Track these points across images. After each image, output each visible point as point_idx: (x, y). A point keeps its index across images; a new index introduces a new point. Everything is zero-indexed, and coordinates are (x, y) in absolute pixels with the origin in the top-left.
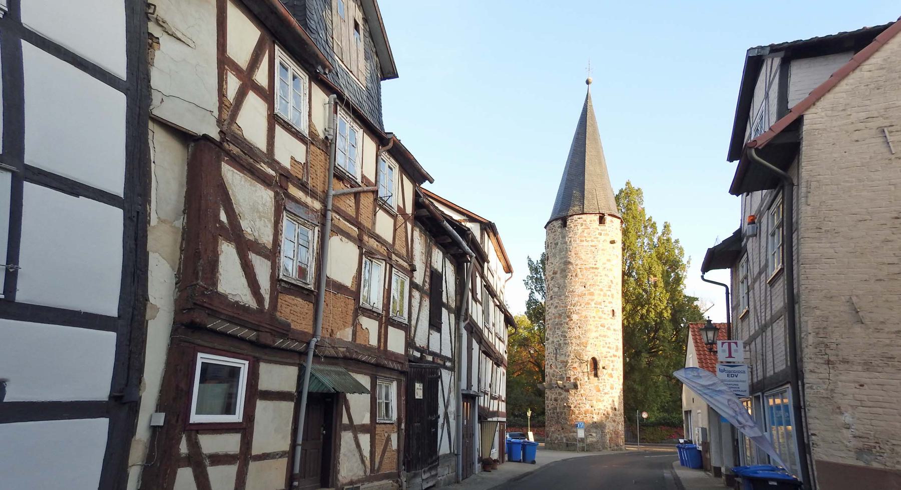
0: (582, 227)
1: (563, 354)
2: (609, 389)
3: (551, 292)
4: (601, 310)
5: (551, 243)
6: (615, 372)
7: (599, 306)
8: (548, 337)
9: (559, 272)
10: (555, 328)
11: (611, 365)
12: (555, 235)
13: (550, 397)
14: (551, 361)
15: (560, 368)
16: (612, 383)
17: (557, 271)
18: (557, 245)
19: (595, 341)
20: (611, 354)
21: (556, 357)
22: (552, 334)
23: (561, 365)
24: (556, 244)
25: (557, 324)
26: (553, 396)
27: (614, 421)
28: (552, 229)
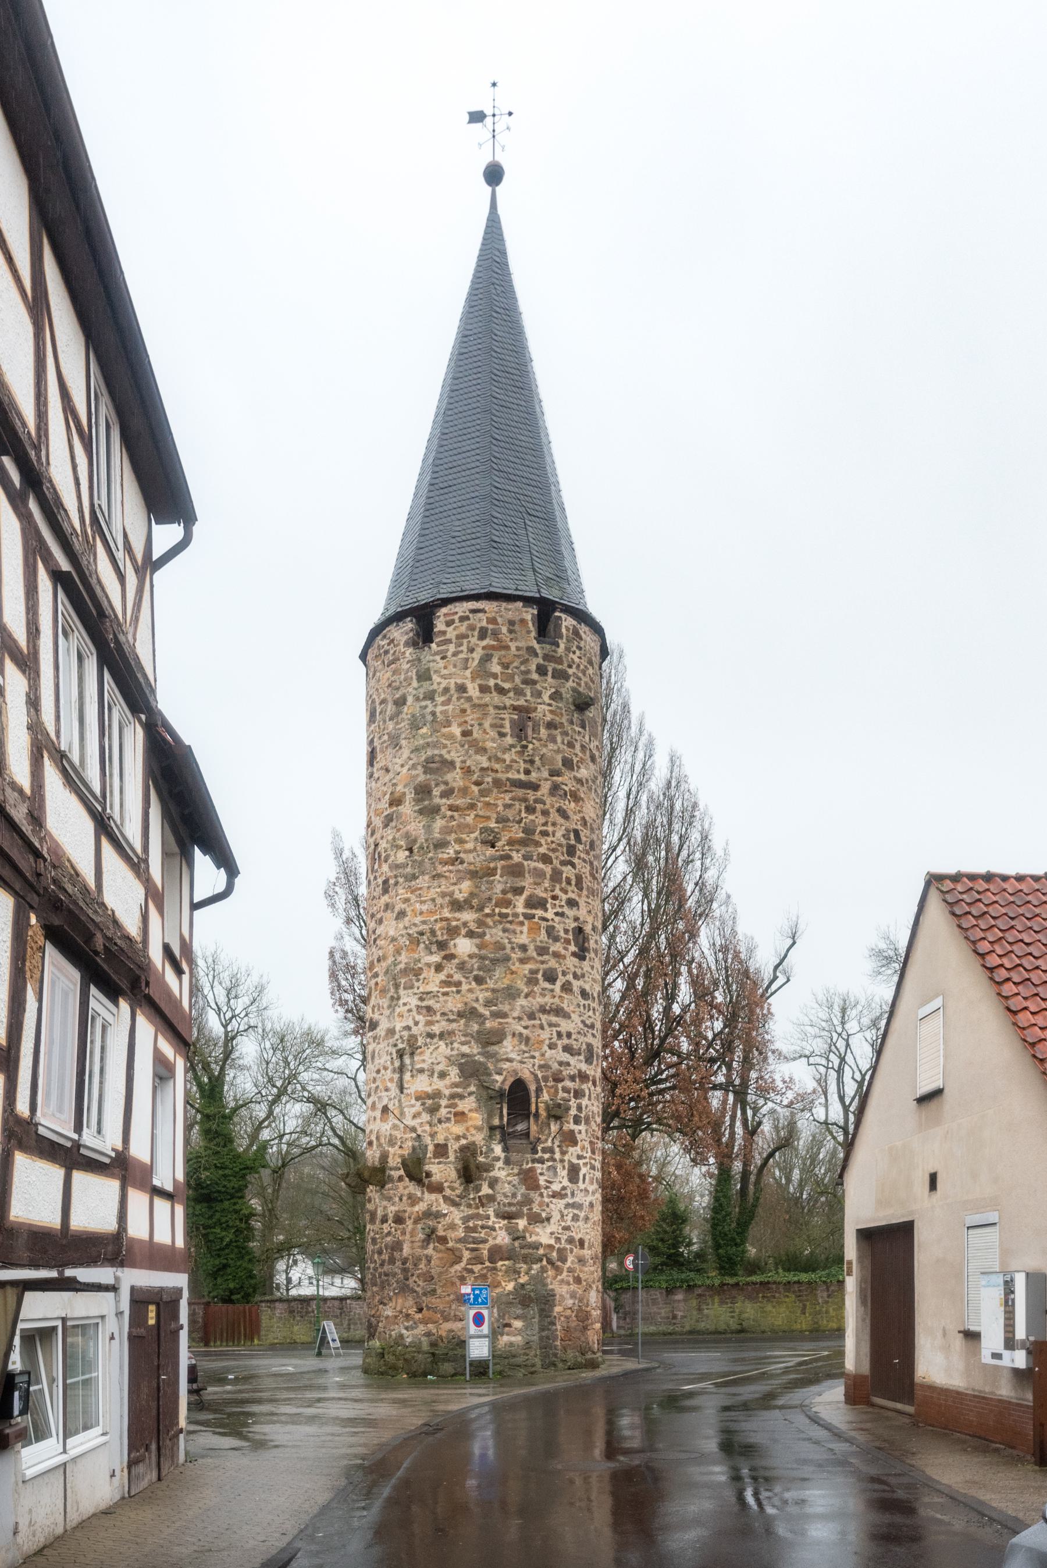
0: (484, 643)
1: (421, 1071)
2: (566, 1182)
3: (385, 868)
4: (544, 924)
5: (383, 702)
6: (582, 1127)
7: (539, 913)
8: (376, 1016)
9: (410, 796)
10: (397, 986)
11: (573, 1103)
12: (394, 673)
13: (380, 1213)
14: (384, 1094)
15: (414, 1117)
16: (575, 1161)
17: (404, 794)
18: (404, 703)
19: (526, 1028)
20: (573, 1071)
21: (401, 1079)
22: (389, 1007)
23: (418, 1107)
24: (401, 702)
25: (405, 971)
26: (392, 1209)
27: (578, 1280)
28: (386, 652)
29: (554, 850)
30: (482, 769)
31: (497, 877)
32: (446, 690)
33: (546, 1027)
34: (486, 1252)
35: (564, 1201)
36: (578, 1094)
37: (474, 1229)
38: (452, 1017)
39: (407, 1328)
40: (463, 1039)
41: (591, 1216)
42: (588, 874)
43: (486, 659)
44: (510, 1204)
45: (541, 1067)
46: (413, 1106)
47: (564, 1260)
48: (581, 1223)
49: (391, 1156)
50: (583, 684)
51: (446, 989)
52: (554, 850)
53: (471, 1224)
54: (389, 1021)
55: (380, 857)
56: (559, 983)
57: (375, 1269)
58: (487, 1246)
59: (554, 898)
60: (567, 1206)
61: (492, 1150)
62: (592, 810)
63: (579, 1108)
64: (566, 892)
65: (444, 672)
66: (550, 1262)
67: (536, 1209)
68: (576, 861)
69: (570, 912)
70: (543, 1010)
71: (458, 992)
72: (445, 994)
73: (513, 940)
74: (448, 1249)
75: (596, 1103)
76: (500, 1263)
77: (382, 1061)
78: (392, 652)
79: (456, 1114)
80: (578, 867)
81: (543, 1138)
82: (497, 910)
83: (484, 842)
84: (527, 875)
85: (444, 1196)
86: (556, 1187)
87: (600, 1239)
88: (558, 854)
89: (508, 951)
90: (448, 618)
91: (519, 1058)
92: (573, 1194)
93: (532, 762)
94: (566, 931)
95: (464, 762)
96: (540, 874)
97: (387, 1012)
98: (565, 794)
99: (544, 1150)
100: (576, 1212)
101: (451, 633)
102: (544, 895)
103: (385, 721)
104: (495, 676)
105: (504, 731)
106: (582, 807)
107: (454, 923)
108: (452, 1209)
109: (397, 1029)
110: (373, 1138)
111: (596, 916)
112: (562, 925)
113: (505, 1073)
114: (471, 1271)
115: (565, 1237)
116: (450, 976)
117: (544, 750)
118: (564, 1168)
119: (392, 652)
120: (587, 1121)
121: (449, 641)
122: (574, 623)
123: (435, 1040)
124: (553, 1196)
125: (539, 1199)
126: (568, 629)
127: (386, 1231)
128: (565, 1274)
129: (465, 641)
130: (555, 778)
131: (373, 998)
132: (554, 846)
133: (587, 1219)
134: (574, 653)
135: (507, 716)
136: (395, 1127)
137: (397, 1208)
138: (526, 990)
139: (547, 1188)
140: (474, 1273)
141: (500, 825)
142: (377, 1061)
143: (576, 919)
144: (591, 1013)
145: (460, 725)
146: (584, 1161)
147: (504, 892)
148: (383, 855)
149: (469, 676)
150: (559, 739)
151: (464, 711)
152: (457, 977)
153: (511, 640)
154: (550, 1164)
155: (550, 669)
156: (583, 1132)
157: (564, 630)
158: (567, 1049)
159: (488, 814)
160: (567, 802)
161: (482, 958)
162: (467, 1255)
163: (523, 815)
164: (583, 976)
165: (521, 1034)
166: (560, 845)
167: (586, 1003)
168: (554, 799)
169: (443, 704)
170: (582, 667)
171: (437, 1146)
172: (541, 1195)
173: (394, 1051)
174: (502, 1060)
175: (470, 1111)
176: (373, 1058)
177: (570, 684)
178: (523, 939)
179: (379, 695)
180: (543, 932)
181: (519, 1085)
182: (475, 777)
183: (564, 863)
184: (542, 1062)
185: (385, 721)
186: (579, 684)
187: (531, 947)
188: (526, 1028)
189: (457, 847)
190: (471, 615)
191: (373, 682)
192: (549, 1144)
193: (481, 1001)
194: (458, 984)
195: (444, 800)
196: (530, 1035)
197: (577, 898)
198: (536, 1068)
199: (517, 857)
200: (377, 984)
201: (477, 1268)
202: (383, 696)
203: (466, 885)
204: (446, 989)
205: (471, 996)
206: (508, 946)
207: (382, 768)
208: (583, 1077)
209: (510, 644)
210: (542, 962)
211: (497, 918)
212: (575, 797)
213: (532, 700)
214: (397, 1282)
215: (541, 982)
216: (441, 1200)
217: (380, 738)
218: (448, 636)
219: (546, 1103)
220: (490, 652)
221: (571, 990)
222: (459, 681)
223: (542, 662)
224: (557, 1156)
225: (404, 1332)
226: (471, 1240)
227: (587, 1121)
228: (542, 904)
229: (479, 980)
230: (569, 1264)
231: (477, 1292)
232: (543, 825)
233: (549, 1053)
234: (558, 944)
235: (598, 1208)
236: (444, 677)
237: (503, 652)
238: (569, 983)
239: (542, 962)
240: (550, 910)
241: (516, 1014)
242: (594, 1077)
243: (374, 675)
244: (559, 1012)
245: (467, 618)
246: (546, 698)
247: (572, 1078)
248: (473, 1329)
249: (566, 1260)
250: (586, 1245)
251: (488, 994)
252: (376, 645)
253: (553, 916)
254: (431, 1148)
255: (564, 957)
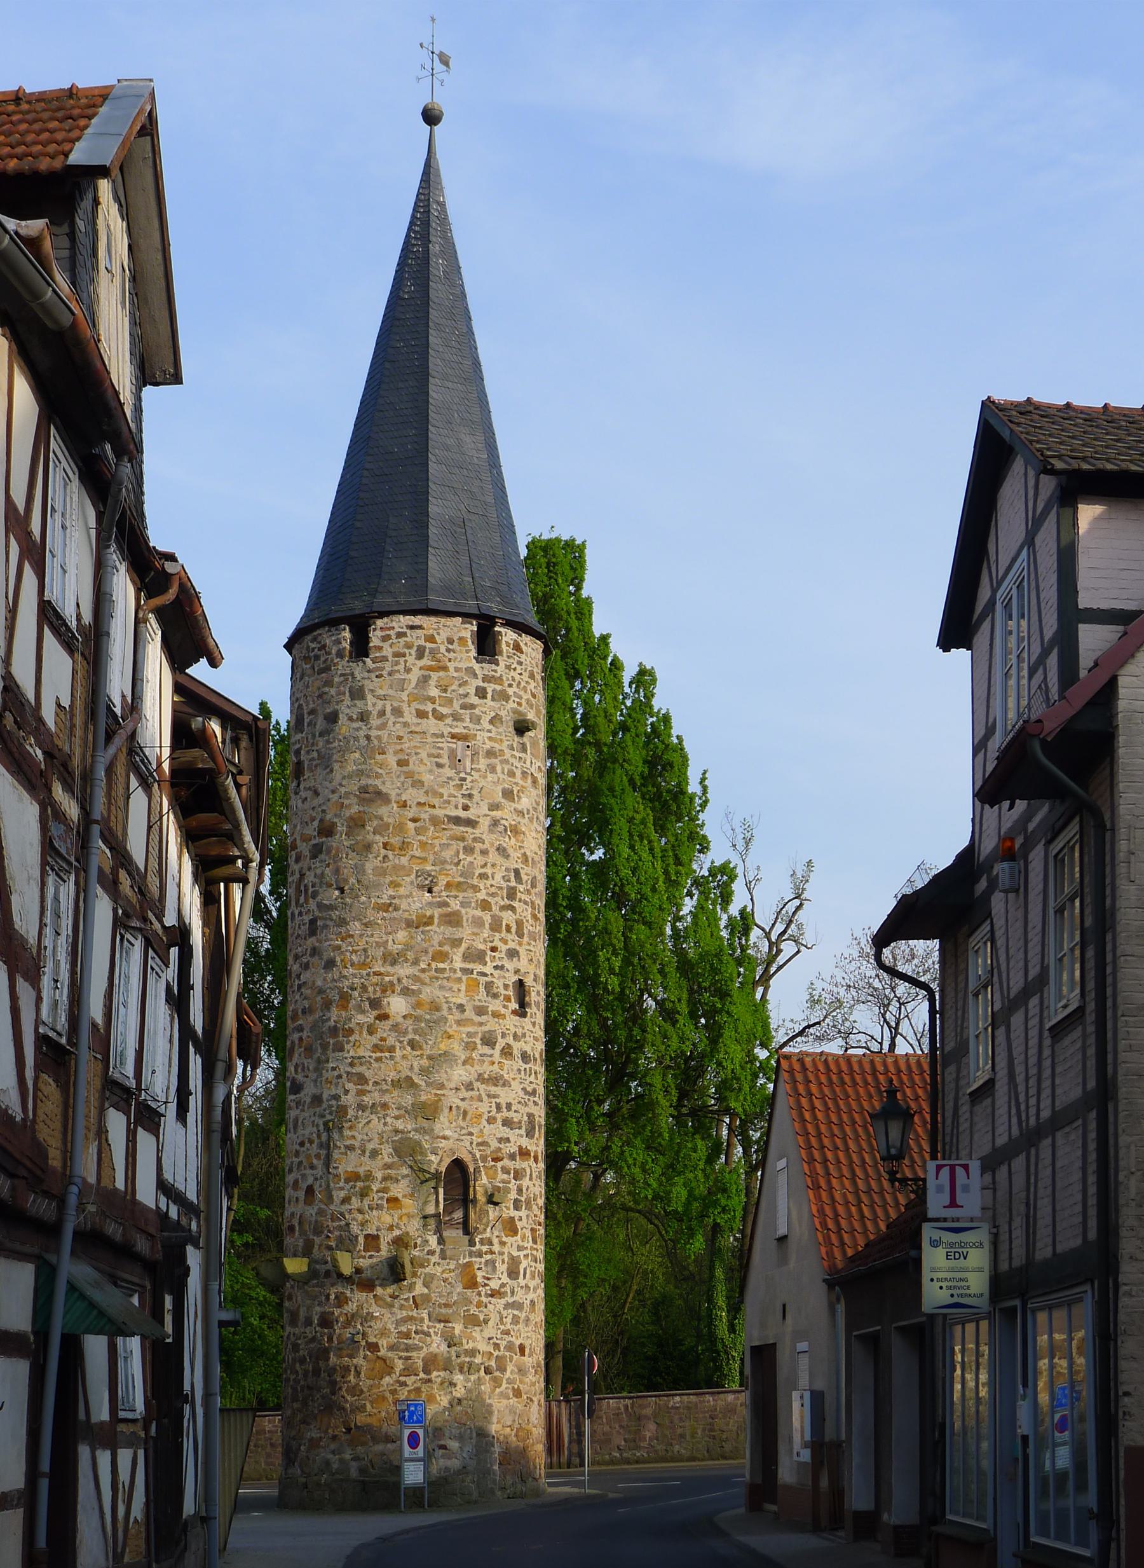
2: (505, 1279)
4: (483, 980)
5: (312, 712)
6: (523, 1213)
7: (478, 968)
8: (300, 1077)
11: (513, 1185)
13: (302, 1314)
14: (308, 1172)
16: (515, 1254)
19: (463, 1100)
20: (514, 1149)
22: (316, 1070)
27: (518, 1393)
28: (317, 657)
29: (493, 895)
30: (419, 804)
31: (434, 928)
32: (382, 713)
33: (485, 1098)
34: (420, 1363)
35: (503, 1301)
36: (518, 1175)
37: (407, 1336)
38: (385, 1087)
39: (333, 1452)
40: (397, 1113)
41: (532, 1317)
42: (529, 917)
43: (425, 680)
44: (446, 1305)
45: (479, 1144)
46: (342, 1189)
47: (502, 1369)
48: (521, 1326)
49: (316, 1247)
50: (524, 702)
51: (379, 1054)
52: (493, 895)
53: (404, 1329)
54: (316, 1086)
55: (306, 891)
56: (498, 1047)
57: (296, 1381)
58: (422, 1354)
59: (494, 949)
60: (507, 1306)
61: (427, 1241)
62: (533, 841)
63: (520, 1191)
64: (505, 942)
65: (381, 692)
66: (488, 1371)
67: (473, 1310)
68: (516, 904)
69: (510, 965)
70: (480, 1078)
71: (392, 1058)
72: (378, 1060)
73: (450, 999)
74: (378, 1357)
75: (538, 1183)
76: (435, 1374)
77: (307, 1132)
78: (322, 659)
79: (388, 1201)
80: (518, 910)
81: (481, 1227)
82: (434, 965)
83: (421, 887)
84: (465, 924)
85: (375, 1296)
86: (494, 1284)
87: (542, 1343)
88: (498, 899)
89: (445, 1012)
90: (383, 634)
91: (456, 1136)
92: (513, 1293)
93: (470, 796)
94: (506, 986)
95: (399, 795)
96: (478, 923)
97: (313, 1076)
98: (506, 830)
99: (482, 1242)
100: (516, 1312)
101: (387, 651)
102: (481, 947)
103: (314, 736)
104: (432, 700)
105: (440, 760)
106: (523, 842)
107: (387, 979)
108: (384, 1311)
109: (325, 1096)
110: (295, 1222)
111: (537, 966)
112: (502, 980)
113: (440, 1153)
114: (404, 1384)
115: (504, 1343)
116: (382, 1039)
117: (482, 783)
118: (503, 1262)
119: (322, 659)
120: (529, 1207)
121: (385, 659)
122: (515, 636)
123: (367, 1113)
124: (492, 1296)
125: (476, 1299)
126: (508, 645)
127: (310, 1336)
128: (504, 1385)
129: (402, 660)
130: (494, 813)
131: (296, 1055)
132: (493, 890)
133: (527, 1320)
134: (515, 669)
135: (445, 745)
136: (321, 1212)
137: (322, 1310)
138: (463, 1057)
139: (486, 1285)
140: (406, 1385)
141: (437, 868)
142: (300, 1131)
143: (517, 972)
144: (532, 1079)
145: (396, 753)
146: (525, 1252)
147: (441, 944)
148: (311, 890)
149: (406, 699)
150: (499, 768)
151: (400, 738)
152: (391, 1041)
153: (450, 660)
154: (489, 1257)
155: (489, 691)
156: (524, 1218)
157: (504, 646)
158: (507, 1123)
159: (423, 855)
160: (507, 839)
161: (417, 1019)
162: (399, 1365)
163: (461, 856)
164: (524, 1035)
165: (458, 1107)
166: (501, 888)
167: (527, 1066)
168: (493, 836)
169: (379, 728)
170: (523, 684)
171: (367, 1237)
172: (479, 1294)
173: (321, 1123)
174: (438, 1137)
175: (405, 1196)
176: (295, 1127)
177: (511, 705)
178: (461, 999)
179: (308, 704)
180: (482, 989)
181: (458, 1165)
182: (410, 814)
183: (503, 908)
184: (480, 1140)
185: (314, 736)
186: (519, 704)
187: (469, 1008)
188: (463, 1100)
189: (391, 892)
190: (408, 632)
191: (300, 685)
192: (488, 1234)
193: (416, 1070)
194: (392, 1049)
195: (377, 837)
196: (468, 1109)
197: (518, 948)
198: (474, 1145)
199: (455, 905)
200: (301, 1039)
201: (410, 1380)
202: (311, 706)
203: (402, 935)
204: (379, 1054)
205: (405, 1063)
206: (445, 1007)
207: (310, 788)
208: (524, 1153)
209: (449, 664)
210: (481, 1024)
211: (433, 972)
212: (516, 831)
213: (471, 726)
214: (323, 1397)
215: (479, 1046)
216: (373, 1301)
217: (308, 752)
218: (384, 653)
219: (484, 1186)
220: (426, 673)
221: (511, 1054)
222: (395, 704)
223: (482, 684)
224: (496, 1248)
225: (330, 1456)
226: (402, 1346)
227: (529, 1207)
228: (480, 957)
229: (413, 1045)
230: (508, 1374)
231: (412, 1408)
232: (482, 867)
233: (488, 1129)
234: (497, 1002)
235: (541, 1306)
236: (378, 697)
237: (441, 674)
238: (509, 1046)
239: (481, 1024)
240: (489, 963)
241: (453, 1085)
242: (536, 1152)
243: (301, 679)
244: (495, 1080)
245: (404, 634)
246: (485, 724)
247: (512, 1157)
248: (407, 1451)
249: (505, 1370)
250: (527, 1352)
251: (425, 1062)
252: (304, 644)
253: (493, 971)
254: (361, 1240)
255: (504, 1017)
